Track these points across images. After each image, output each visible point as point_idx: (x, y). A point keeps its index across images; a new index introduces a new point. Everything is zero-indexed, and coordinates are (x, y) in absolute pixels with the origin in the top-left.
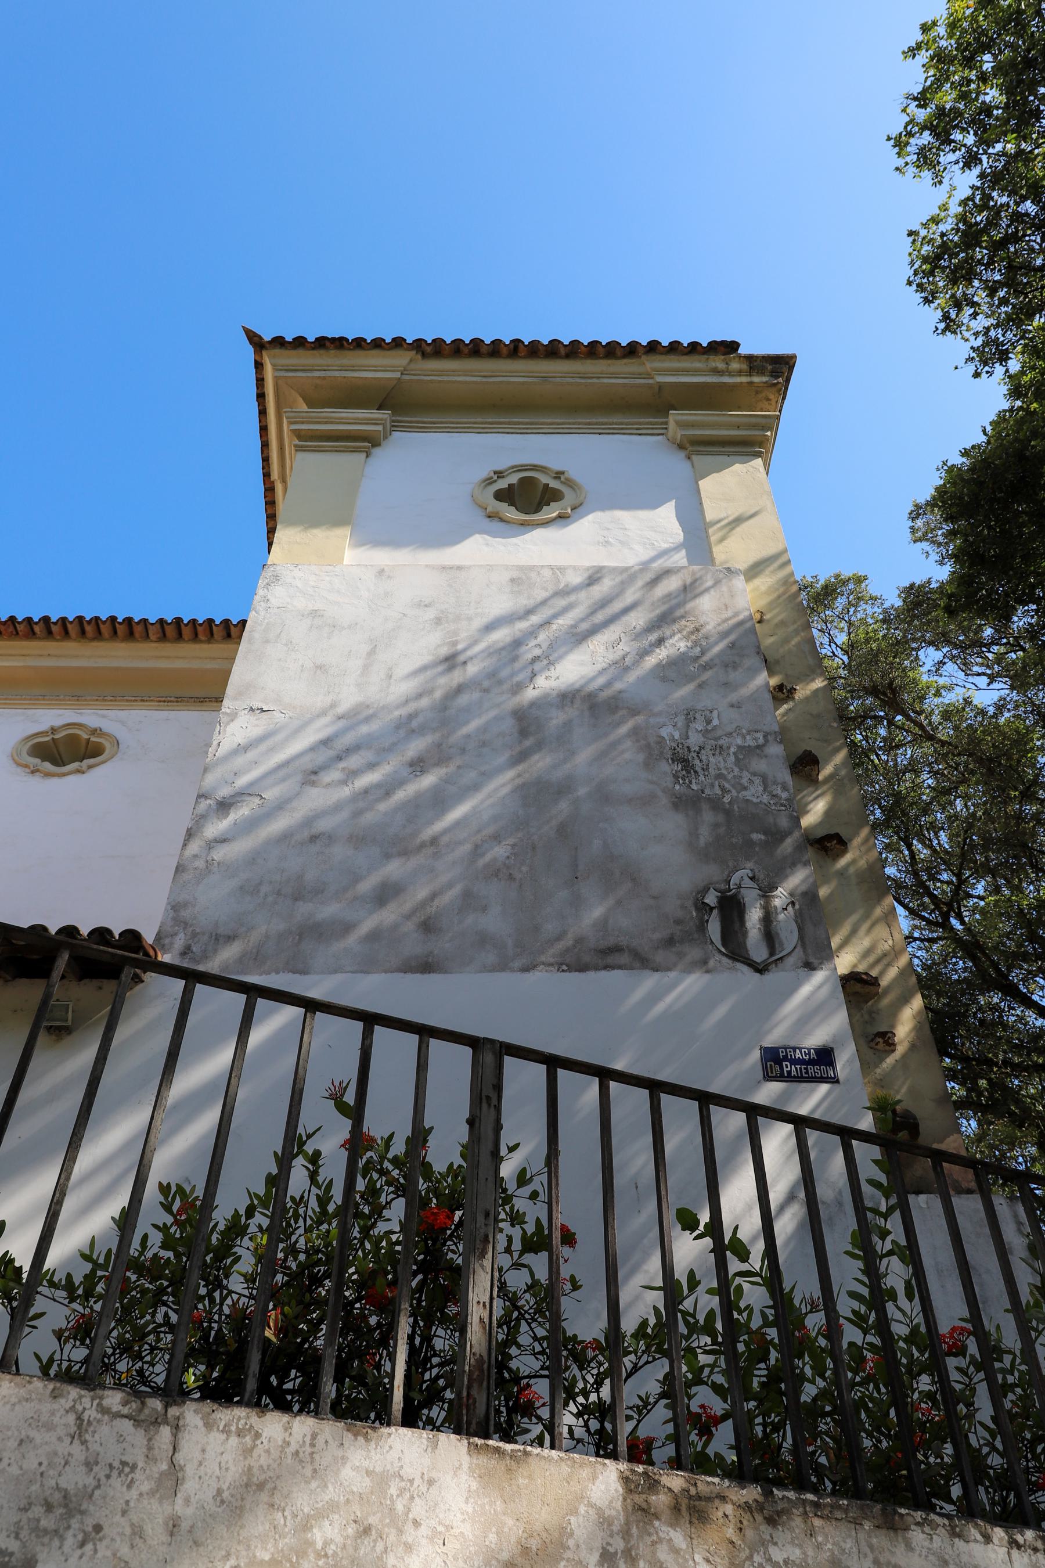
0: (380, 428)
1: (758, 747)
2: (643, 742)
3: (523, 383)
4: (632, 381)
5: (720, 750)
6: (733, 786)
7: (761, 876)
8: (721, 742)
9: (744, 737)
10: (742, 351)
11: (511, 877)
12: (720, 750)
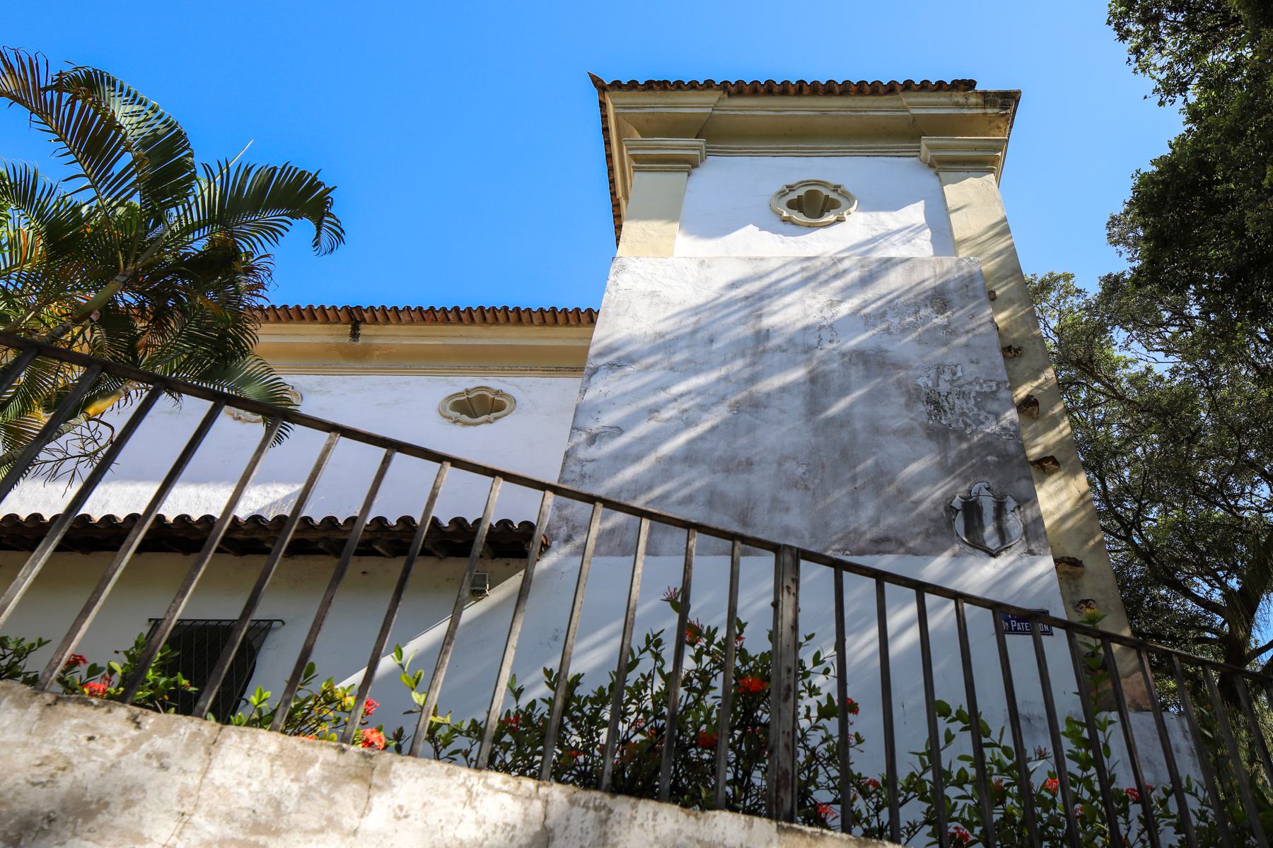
0: (697, 153)
1: (993, 393)
2: (904, 389)
3: (808, 116)
4: (892, 114)
5: (963, 395)
6: (974, 421)
7: (995, 487)
8: (964, 389)
9: (981, 385)
10: (978, 88)
11: (807, 488)
12: (963, 395)
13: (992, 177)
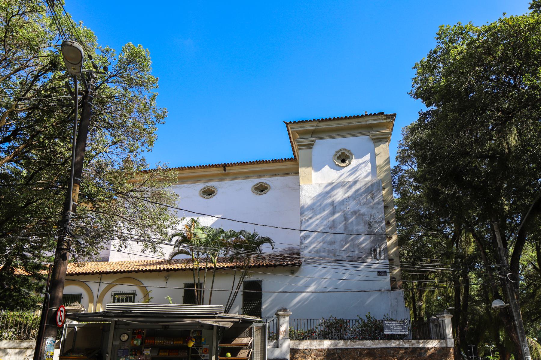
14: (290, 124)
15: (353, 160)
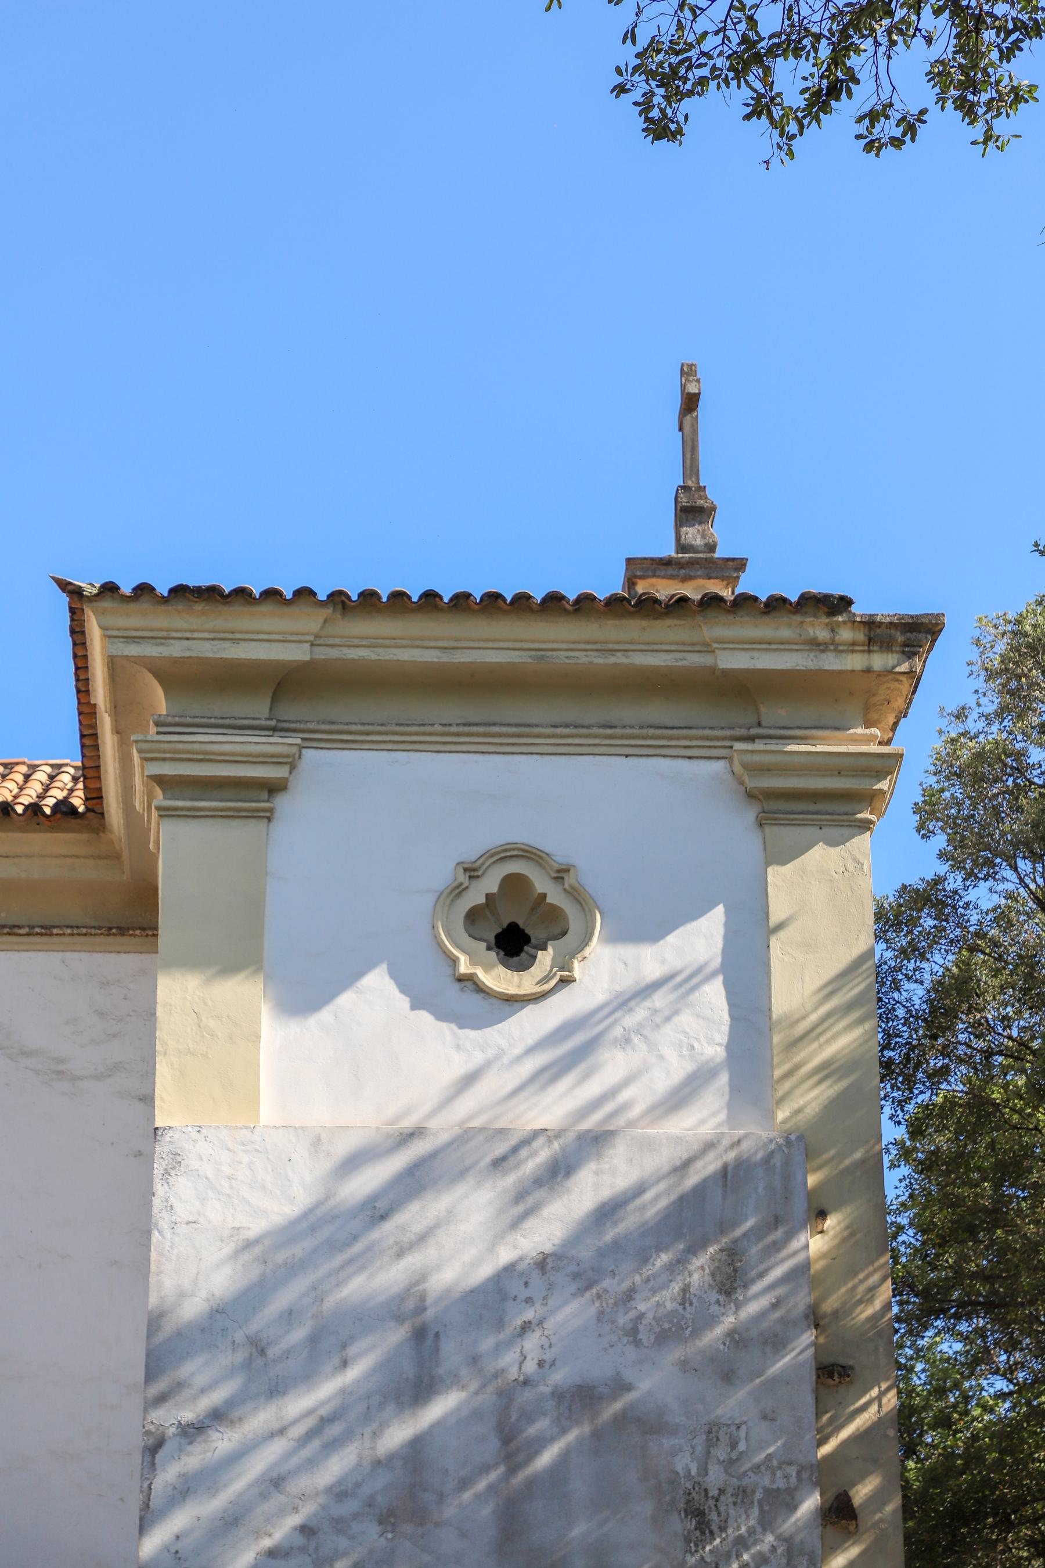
8: (746, 1481)
13: (868, 833)
14: (106, 604)
15: (596, 948)
